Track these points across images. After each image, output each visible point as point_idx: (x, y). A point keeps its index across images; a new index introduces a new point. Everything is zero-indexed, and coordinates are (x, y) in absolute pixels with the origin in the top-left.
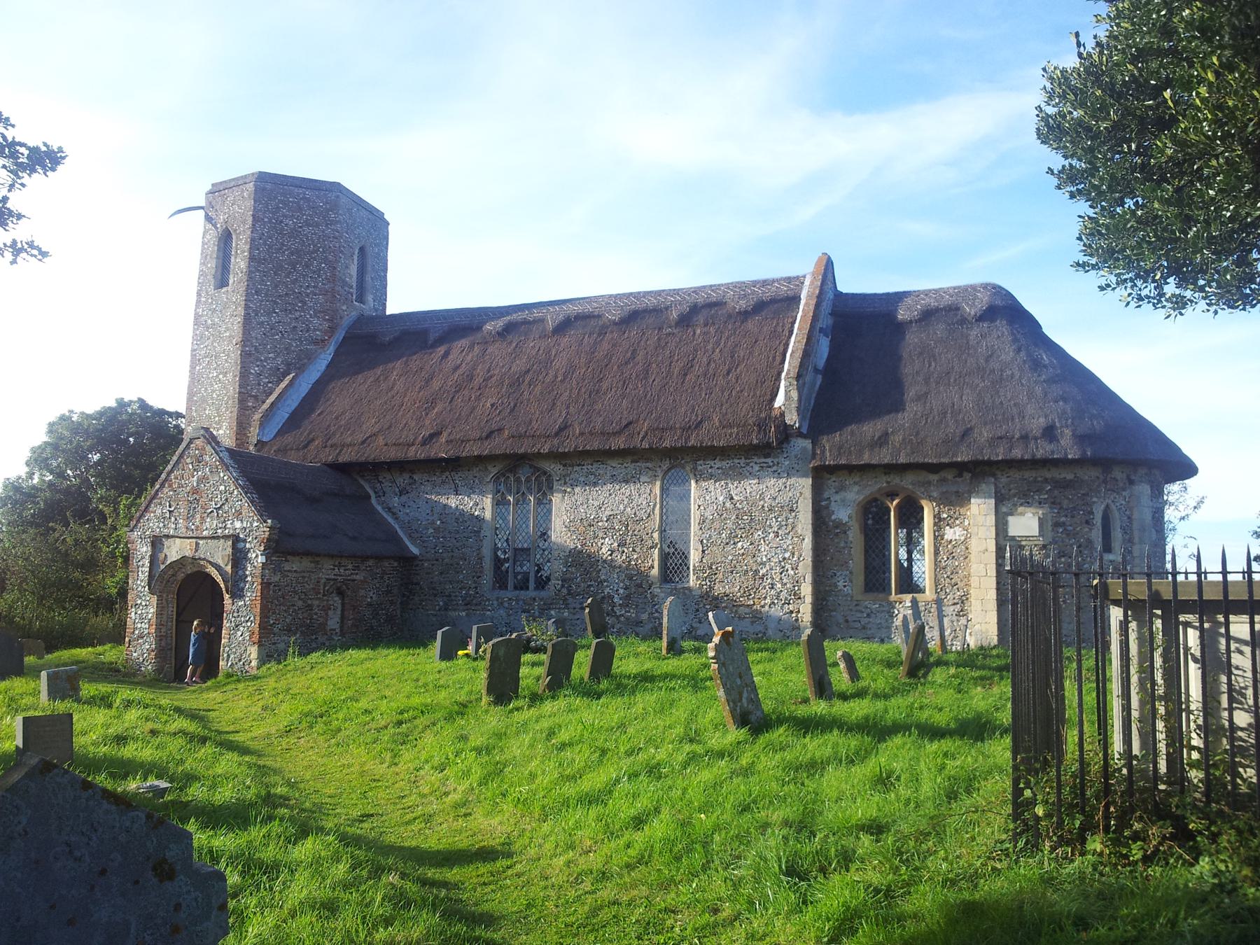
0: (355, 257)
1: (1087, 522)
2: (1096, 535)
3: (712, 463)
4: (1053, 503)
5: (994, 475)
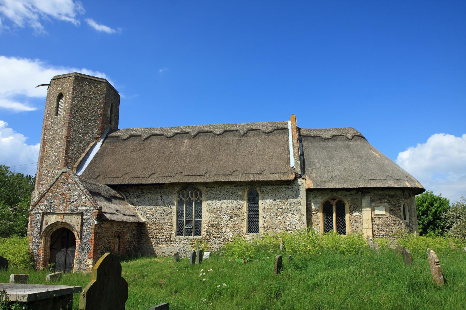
1: (399, 209)
3: (267, 187)
4: (389, 203)
5: (369, 193)
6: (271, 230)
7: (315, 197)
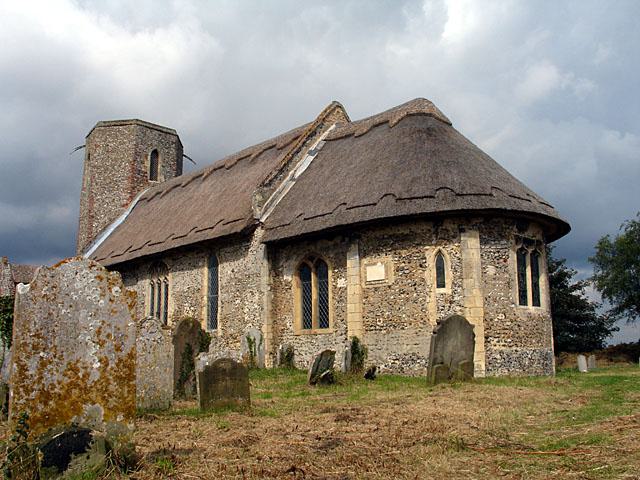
0: (149, 157)
1: (421, 266)
2: (430, 275)
5: (359, 237)
7: (288, 259)
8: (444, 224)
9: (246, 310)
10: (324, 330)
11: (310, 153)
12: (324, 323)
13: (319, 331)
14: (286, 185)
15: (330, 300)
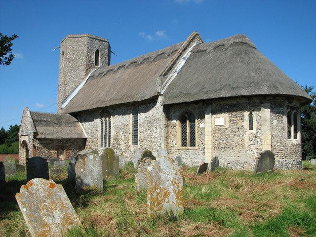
0: (94, 54)
2: (246, 123)
6: (144, 142)
7: (175, 112)
8: (252, 102)
9: (153, 136)
10: (193, 148)
11: (184, 58)
12: (193, 144)
13: (190, 148)
14: (173, 75)
15: (196, 134)
